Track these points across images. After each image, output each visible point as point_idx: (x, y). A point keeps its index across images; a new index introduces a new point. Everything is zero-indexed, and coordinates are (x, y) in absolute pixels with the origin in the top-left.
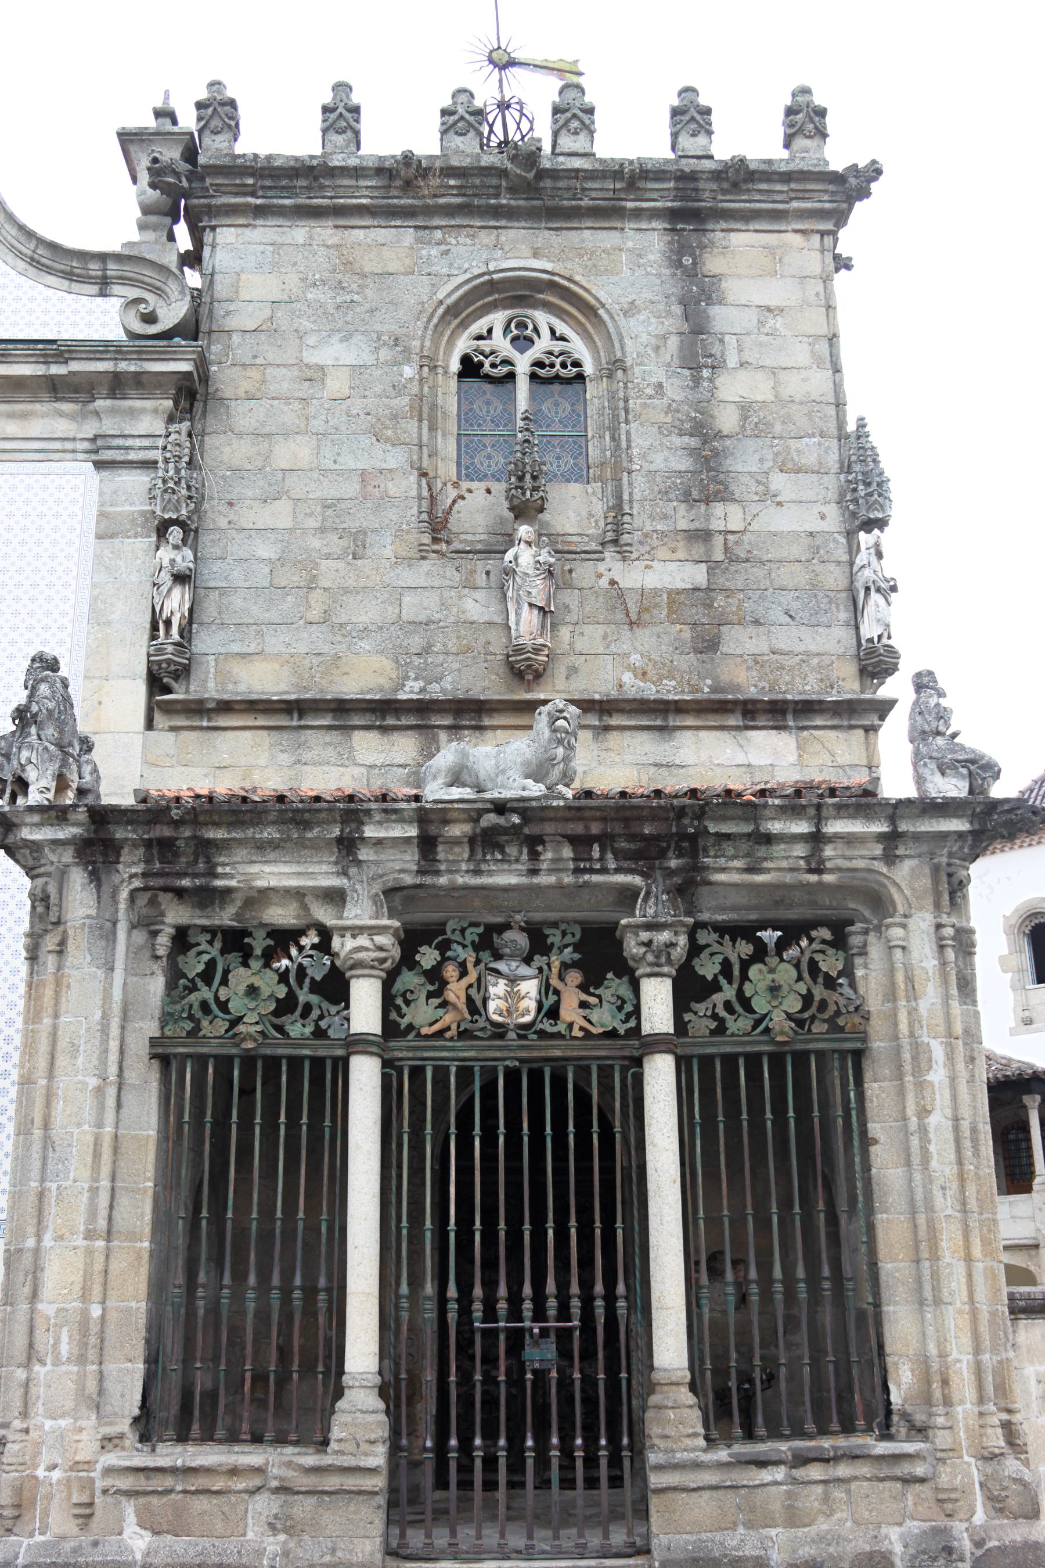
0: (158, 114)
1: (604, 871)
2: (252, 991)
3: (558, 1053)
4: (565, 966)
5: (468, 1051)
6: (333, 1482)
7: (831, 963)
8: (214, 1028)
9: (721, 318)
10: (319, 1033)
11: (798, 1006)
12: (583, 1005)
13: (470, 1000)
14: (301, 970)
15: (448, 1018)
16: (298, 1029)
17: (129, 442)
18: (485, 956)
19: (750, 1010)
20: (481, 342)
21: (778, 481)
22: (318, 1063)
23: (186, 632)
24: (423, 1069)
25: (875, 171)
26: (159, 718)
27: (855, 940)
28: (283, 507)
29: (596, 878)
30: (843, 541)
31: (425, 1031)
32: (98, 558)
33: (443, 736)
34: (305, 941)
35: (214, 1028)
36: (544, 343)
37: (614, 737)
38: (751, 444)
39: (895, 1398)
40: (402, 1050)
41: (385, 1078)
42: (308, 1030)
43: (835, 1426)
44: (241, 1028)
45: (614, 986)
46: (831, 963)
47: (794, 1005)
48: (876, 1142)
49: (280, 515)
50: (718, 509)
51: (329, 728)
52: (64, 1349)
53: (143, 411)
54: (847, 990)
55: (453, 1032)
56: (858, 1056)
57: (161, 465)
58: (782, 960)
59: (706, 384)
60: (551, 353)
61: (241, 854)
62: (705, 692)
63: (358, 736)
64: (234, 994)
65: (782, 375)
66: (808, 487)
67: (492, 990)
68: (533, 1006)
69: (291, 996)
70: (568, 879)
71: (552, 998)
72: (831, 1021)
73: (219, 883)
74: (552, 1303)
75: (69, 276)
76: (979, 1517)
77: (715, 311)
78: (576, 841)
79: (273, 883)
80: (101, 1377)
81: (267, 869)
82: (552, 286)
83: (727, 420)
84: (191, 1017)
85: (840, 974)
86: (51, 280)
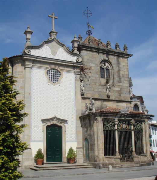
6: (117, 158)
9: (121, 66)
16: (112, 128)
21: (125, 81)
25: (132, 55)
35: (107, 128)
36: (106, 65)
38: (123, 78)
39: (144, 152)
45: (130, 126)
50: (121, 83)
56: (143, 131)
62: (120, 100)
76: (149, 159)
83: (121, 75)
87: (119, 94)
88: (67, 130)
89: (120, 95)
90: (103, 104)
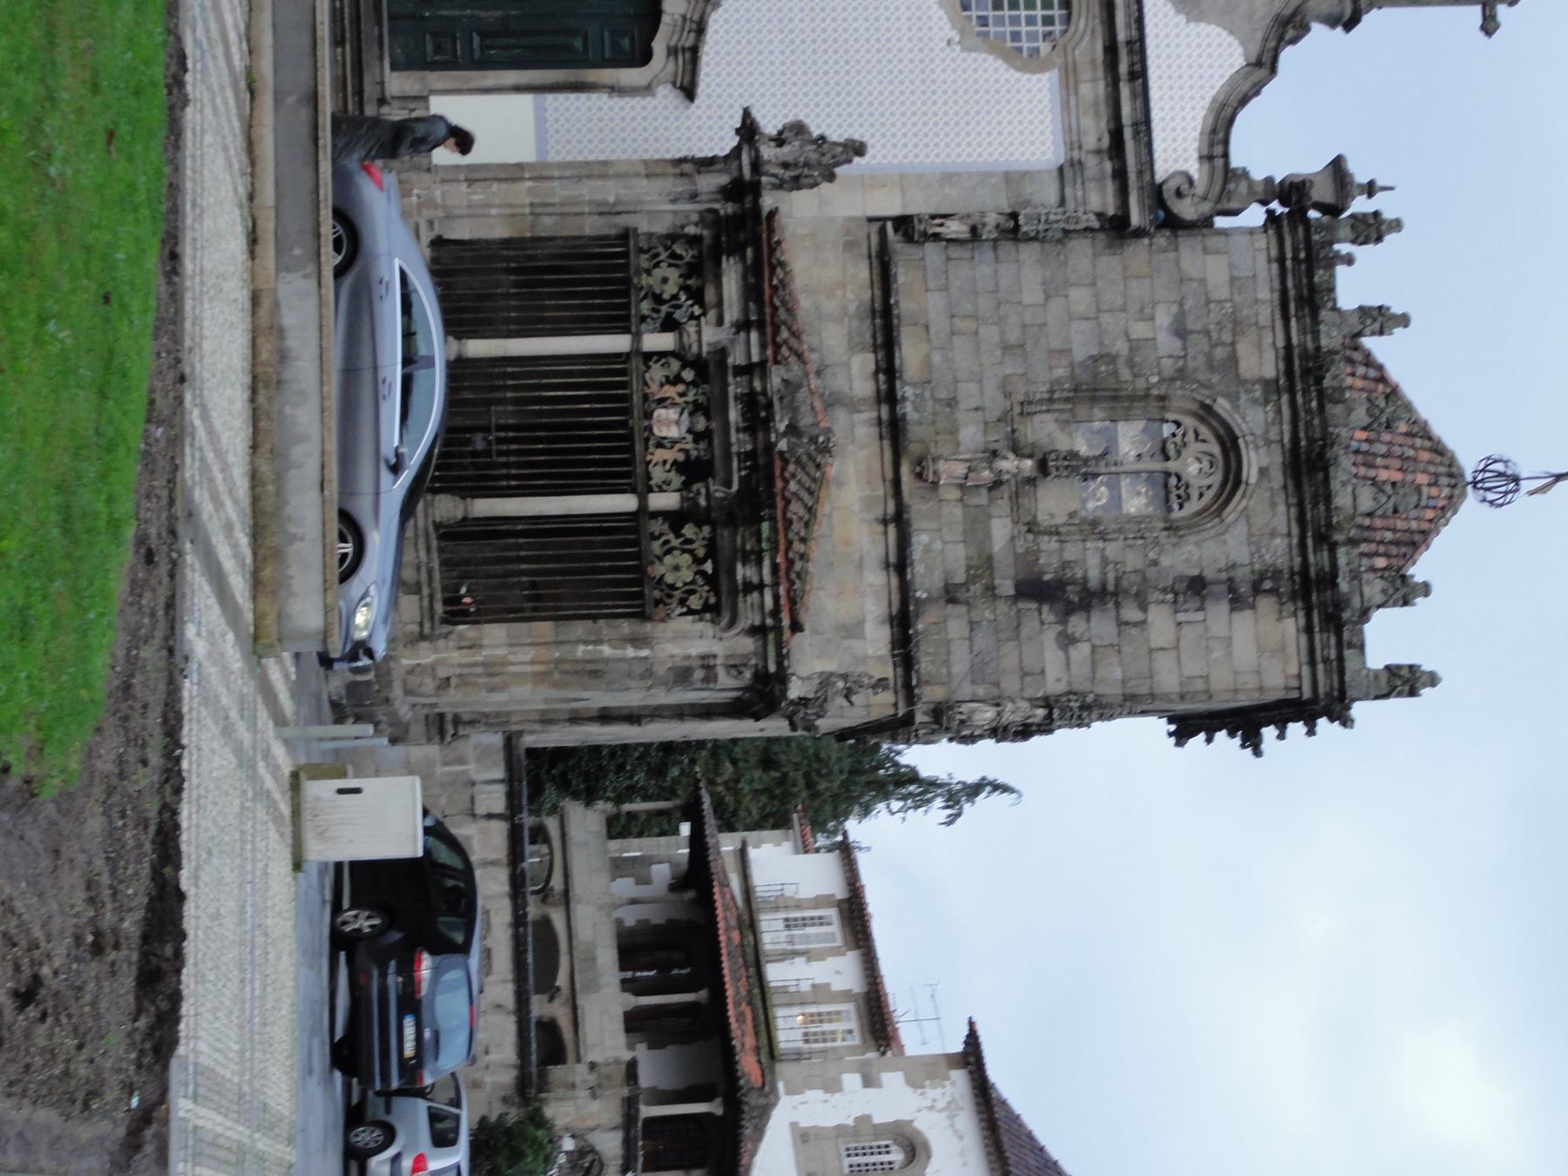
0: (1371, 184)
1: (740, 469)
2: (665, 280)
5: (636, 399)
7: (695, 602)
8: (644, 261)
10: (643, 319)
12: (665, 462)
14: (679, 307)
15: (654, 387)
16: (645, 307)
17: (1079, 186)
18: (690, 407)
20: (1191, 436)
22: (627, 318)
23: (936, 237)
27: (708, 616)
28: (1040, 297)
29: (735, 464)
30: (1039, 695)
32: (990, 174)
33: (874, 414)
35: (644, 261)
37: (881, 528)
39: (461, 627)
40: (636, 363)
41: (618, 355)
45: (677, 480)
46: (695, 602)
47: (669, 579)
49: (1032, 293)
51: (874, 337)
52: (475, 197)
53: (1104, 195)
56: (643, 617)
58: (696, 573)
59: (1161, 597)
60: (1187, 487)
61: (740, 267)
63: (870, 357)
64: (663, 271)
66: (1080, 671)
68: (664, 434)
69: (664, 302)
70: (734, 449)
73: (724, 258)
74: (504, 447)
75: (1214, 131)
77: (1224, 607)
78: (754, 451)
80: (462, 217)
82: (1238, 482)
84: (649, 250)
86: (1210, 120)
87: (960, 578)
88: (628, 102)
89: (951, 595)
90: (856, 417)
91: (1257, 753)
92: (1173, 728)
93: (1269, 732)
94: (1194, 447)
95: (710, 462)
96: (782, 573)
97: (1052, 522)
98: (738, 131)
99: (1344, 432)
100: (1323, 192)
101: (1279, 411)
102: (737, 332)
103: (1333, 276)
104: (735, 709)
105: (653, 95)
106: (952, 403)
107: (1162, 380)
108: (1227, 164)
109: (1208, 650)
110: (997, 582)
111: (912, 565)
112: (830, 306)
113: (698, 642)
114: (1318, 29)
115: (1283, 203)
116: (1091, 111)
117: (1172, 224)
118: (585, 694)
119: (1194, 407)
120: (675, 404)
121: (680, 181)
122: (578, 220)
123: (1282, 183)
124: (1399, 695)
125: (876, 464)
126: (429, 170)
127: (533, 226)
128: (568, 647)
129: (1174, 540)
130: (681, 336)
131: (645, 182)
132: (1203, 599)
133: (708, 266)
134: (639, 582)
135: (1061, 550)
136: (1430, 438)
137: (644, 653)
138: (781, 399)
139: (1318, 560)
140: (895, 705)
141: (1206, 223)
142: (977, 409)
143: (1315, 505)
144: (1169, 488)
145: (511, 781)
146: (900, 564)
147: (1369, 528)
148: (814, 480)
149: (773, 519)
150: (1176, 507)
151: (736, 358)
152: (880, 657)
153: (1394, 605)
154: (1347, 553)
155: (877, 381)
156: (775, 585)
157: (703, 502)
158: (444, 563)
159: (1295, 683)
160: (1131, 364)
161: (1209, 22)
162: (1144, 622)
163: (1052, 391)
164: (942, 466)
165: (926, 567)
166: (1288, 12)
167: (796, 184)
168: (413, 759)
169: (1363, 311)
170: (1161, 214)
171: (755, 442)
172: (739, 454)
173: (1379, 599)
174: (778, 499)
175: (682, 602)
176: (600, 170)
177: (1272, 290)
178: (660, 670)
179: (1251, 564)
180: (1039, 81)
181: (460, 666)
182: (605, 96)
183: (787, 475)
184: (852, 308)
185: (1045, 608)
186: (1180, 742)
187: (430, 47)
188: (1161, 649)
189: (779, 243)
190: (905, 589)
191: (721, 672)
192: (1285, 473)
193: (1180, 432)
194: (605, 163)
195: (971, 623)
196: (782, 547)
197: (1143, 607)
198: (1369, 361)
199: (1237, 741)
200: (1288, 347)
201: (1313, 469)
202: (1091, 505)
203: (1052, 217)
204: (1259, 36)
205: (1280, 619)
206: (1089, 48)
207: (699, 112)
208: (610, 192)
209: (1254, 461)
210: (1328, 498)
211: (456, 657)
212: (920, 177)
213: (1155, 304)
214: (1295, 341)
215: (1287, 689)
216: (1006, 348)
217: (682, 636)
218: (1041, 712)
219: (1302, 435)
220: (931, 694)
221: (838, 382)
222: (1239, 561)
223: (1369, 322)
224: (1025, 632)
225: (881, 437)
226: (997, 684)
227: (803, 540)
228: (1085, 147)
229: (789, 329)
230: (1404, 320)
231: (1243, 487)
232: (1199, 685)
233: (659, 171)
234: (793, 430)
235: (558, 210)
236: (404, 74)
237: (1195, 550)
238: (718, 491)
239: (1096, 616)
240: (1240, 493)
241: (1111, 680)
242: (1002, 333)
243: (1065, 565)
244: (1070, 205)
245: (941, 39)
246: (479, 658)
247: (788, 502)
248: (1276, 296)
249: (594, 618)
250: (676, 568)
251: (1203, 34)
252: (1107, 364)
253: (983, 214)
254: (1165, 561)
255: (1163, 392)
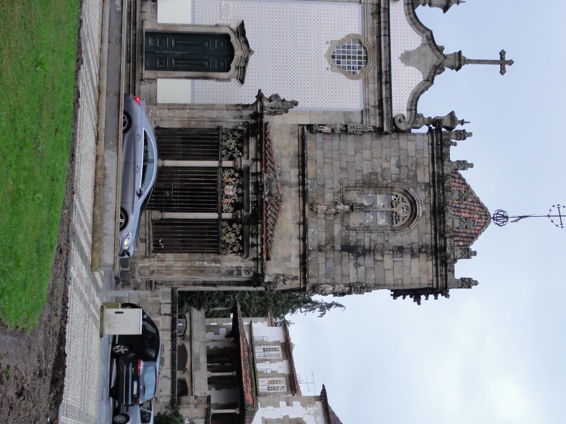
1: (252, 206)
2: (231, 144)
3: (219, 198)
4: (235, 200)
7: (235, 249)
8: (224, 137)
9: (407, 258)
10: (223, 156)
11: (227, 242)
13: (229, 182)
14: (235, 153)
15: (225, 179)
16: (224, 152)
18: (237, 185)
19: (226, 233)
20: (401, 200)
22: (218, 156)
23: (320, 132)
24: (216, 174)
26: (301, 127)
27: (239, 254)
28: (353, 153)
29: (251, 205)
31: (223, 175)
32: (339, 112)
33: (298, 189)
34: (240, 153)
35: (224, 137)
37: (298, 226)
39: (159, 254)
40: (220, 170)
41: (215, 167)
42: (224, 154)
43: (154, 243)
44: (224, 142)
45: (231, 209)
46: (235, 249)
47: (227, 241)
48: (202, 254)
49: (351, 152)
52: (170, 114)
53: (376, 120)
54: (230, 252)
55: (223, 179)
56: (218, 253)
57: (361, 125)
58: (236, 240)
59: (389, 252)
60: (399, 216)
61: (255, 141)
63: (298, 170)
65: (392, 271)
67: (231, 186)
68: (228, 194)
69: (230, 151)
70: (251, 200)
71: (229, 197)
72: (224, 248)
73: (250, 137)
74: (176, 196)
75: (412, 102)
77: (409, 256)
78: (257, 200)
79: (250, 146)
80: (165, 120)
81: (253, 146)
84: (226, 133)
85: (233, 251)
86: (411, 98)
87: (323, 243)
88: (222, 83)
89: (320, 249)
90: (291, 189)
91: (419, 303)
92: (392, 293)
93: (423, 297)
94: (401, 204)
95: (243, 203)
96: (264, 241)
97: (354, 226)
98: (256, 97)
99: (450, 201)
100: (447, 123)
101: (430, 193)
102: (253, 162)
103: (449, 150)
104: (247, 283)
105: (230, 82)
106: (323, 186)
107: (392, 182)
108: (416, 112)
109: (403, 270)
110: (335, 245)
111: (308, 239)
112: (285, 153)
113: (236, 262)
114: (447, 69)
115: (434, 126)
116: (373, 93)
117: (398, 131)
118: (198, 277)
119: (402, 191)
120: (232, 184)
121: (236, 112)
122: (204, 123)
123: (433, 119)
124: (465, 288)
125: (298, 205)
126: (155, 105)
127: (189, 124)
128: (193, 262)
129: (393, 234)
130: (235, 162)
131: (226, 112)
132: (402, 254)
133: (245, 139)
134: (217, 242)
135: (357, 235)
136: (479, 203)
137: (218, 265)
138: (267, 184)
139: (440, 242)
140: (300, 284)
141: (409, 131)
142: (331, 188)
143: (440, 225)
144: (393, 217)
145: (173, 303)
146: (304, 238)
147: (458, 232)
148: (277, 210)
149: (262, 223)
150: (395, 223)
151: (253, 170)
152: (296, 268)
153: (464, 258)
154: (450, 241)
155: (299, 178)
156: (262, 245)
157: (239, 217)
158: (153, 233)
159: (431, 283)
160: (382, 176)
161: (412, 66)
162: (383, 260)
163: (356, 184)
164: (319, 206)
165: (312, 240)
166: (438, 64)
167: (275, 113)
168: (141, 295)
169: (458, 162)
170: (394, 127)
171: (257, 198)
172: (252, 201)
173: (460, 256)
174: (264, 216)
175: (231, 249)
176: (211, 107)
177: (429, 154)
178: (223, 271)
179: (419, 243)
180: (356, 82)
181: (157, 267)
182: (214, 81)
183: (267, 209)
184: (292, 154)
185: (351, 254)
186: (395, 298)
187: (158, 62)
188: (388, 269)
189: (268, 133)
190: (305, 246)
191: (243, 272)
192: (431, 213)
193: (397, 199)
194: (213, 105)
195: (326, 258)
196: (265, 232)
197: (383, 256)
198: (460, 177)
199: (413, 299)
200: (434, 173)
201: (440, 213)
202: (367, 221)
203: (358, 127)
204: (428, 71)
205: (427, 261)
206: (373, 72)
207: (244, 88)
208: (214, 114)
209: (421, 209)
210: (444, 222)
211: (156, 264)
212: (316, 112)
213: (391, 156)
214: (436, 171)
215: (428, 284)
216: (342, 169)
217: (231, 260)
218: (348, 289)
219: (437, 201)
220: (312, 281)
221: (286, 178)
222: (415, 242)
223: (460, 165)
224: (344, 262)
225: (299, 196)
226: (334, 279)
227: (272, 230)
228: (370, 105)
229: (270, 161)
230: (471, 166)
231: (417, 217)
232: (400, 282)
233: (230, 108)
234: (270, 194)
235: (197, 119)
236: (149, 71)
237: (400, 238)
238: (245, 213)
239: (367, 258)
240: (416, 219)
241: (371, 278)
242: (341, 164)
243: (358, 241)
244: (365, 123)
245: (325, 68)
246: (164, 264)
247: (267, 218)
248: (430, 156)
249: (202, 253)
250: (230, 238)
251: (410, 70)
252: (374, 176)
253: (336, 125)
254: (390, 241)
255: (392, 185)
